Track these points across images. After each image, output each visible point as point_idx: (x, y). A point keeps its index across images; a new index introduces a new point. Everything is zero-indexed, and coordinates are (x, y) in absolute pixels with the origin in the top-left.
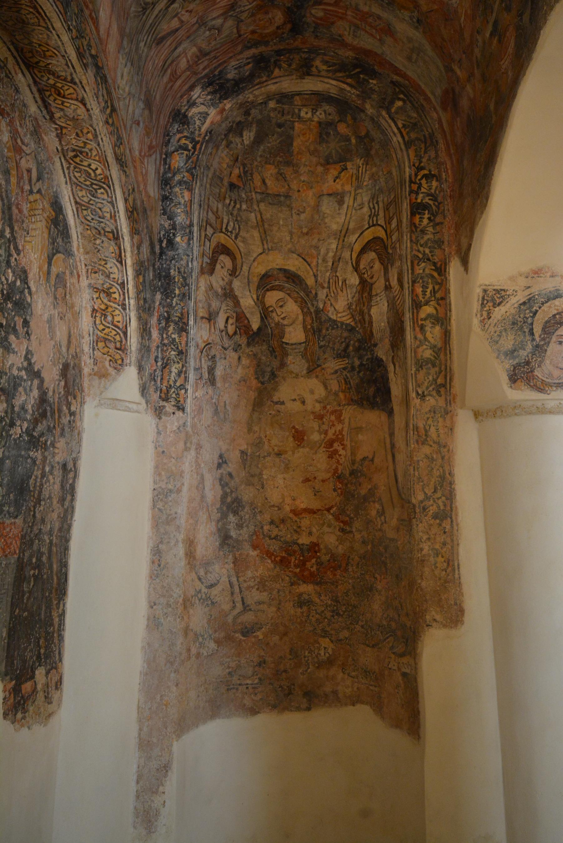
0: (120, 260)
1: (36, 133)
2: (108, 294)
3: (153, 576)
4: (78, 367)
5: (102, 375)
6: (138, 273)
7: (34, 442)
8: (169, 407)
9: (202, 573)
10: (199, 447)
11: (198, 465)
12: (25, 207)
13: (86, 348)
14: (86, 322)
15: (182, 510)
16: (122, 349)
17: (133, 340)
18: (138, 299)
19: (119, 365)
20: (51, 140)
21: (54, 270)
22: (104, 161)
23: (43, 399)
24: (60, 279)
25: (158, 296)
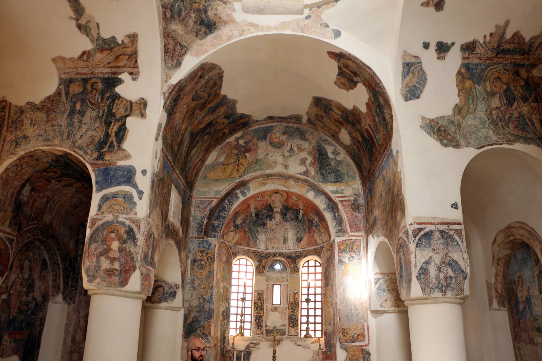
0: (59, 269)
1: (39, 248)
2: (56, 276)
3: (63, 345)
4: (48, 294)
5: (54, 295)
6: (63, 271)
7: (33, 314)
8: (71, 302)
9: (77, 345)
10: (79, 312)
11: (78, 317)
12: (35, 266)
13: (51, 289)
14: (51, 283)
15: (72, 329)
16: (59, 289)
17: (62, 287)
18: (63, 277)
19: (58, 293)
20: (43, 248)
21: (42, 274)
22: (55, 251)
23: (36, 304)
24: (44, 276)
25: (72, 273)
